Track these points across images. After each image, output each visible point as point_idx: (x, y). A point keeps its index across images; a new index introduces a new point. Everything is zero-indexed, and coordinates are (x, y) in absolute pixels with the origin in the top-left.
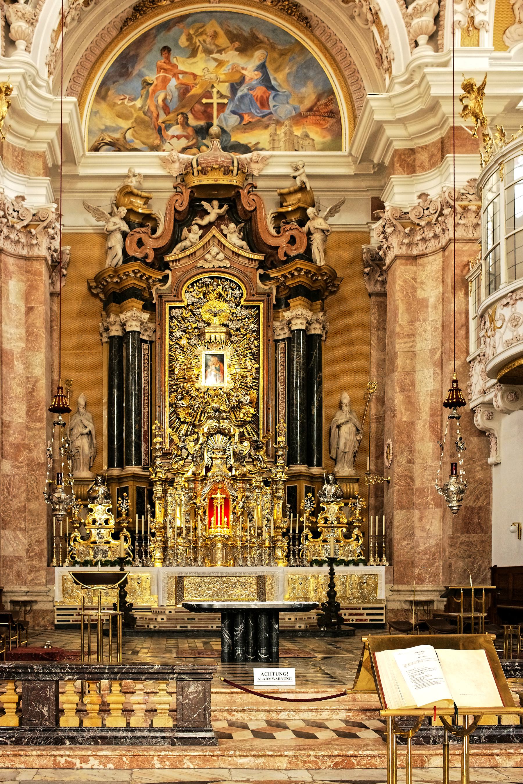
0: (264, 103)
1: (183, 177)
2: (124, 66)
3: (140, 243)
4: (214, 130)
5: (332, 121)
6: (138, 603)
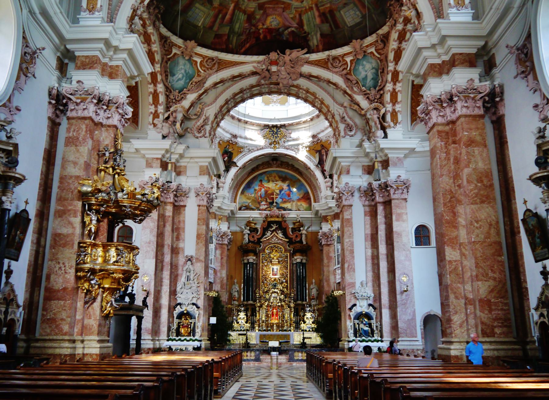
0: (289, 196)
1: (266, 218)
2: (249, 186)
3: (253, 237)
4: (275, 204)
6: (252, 342)
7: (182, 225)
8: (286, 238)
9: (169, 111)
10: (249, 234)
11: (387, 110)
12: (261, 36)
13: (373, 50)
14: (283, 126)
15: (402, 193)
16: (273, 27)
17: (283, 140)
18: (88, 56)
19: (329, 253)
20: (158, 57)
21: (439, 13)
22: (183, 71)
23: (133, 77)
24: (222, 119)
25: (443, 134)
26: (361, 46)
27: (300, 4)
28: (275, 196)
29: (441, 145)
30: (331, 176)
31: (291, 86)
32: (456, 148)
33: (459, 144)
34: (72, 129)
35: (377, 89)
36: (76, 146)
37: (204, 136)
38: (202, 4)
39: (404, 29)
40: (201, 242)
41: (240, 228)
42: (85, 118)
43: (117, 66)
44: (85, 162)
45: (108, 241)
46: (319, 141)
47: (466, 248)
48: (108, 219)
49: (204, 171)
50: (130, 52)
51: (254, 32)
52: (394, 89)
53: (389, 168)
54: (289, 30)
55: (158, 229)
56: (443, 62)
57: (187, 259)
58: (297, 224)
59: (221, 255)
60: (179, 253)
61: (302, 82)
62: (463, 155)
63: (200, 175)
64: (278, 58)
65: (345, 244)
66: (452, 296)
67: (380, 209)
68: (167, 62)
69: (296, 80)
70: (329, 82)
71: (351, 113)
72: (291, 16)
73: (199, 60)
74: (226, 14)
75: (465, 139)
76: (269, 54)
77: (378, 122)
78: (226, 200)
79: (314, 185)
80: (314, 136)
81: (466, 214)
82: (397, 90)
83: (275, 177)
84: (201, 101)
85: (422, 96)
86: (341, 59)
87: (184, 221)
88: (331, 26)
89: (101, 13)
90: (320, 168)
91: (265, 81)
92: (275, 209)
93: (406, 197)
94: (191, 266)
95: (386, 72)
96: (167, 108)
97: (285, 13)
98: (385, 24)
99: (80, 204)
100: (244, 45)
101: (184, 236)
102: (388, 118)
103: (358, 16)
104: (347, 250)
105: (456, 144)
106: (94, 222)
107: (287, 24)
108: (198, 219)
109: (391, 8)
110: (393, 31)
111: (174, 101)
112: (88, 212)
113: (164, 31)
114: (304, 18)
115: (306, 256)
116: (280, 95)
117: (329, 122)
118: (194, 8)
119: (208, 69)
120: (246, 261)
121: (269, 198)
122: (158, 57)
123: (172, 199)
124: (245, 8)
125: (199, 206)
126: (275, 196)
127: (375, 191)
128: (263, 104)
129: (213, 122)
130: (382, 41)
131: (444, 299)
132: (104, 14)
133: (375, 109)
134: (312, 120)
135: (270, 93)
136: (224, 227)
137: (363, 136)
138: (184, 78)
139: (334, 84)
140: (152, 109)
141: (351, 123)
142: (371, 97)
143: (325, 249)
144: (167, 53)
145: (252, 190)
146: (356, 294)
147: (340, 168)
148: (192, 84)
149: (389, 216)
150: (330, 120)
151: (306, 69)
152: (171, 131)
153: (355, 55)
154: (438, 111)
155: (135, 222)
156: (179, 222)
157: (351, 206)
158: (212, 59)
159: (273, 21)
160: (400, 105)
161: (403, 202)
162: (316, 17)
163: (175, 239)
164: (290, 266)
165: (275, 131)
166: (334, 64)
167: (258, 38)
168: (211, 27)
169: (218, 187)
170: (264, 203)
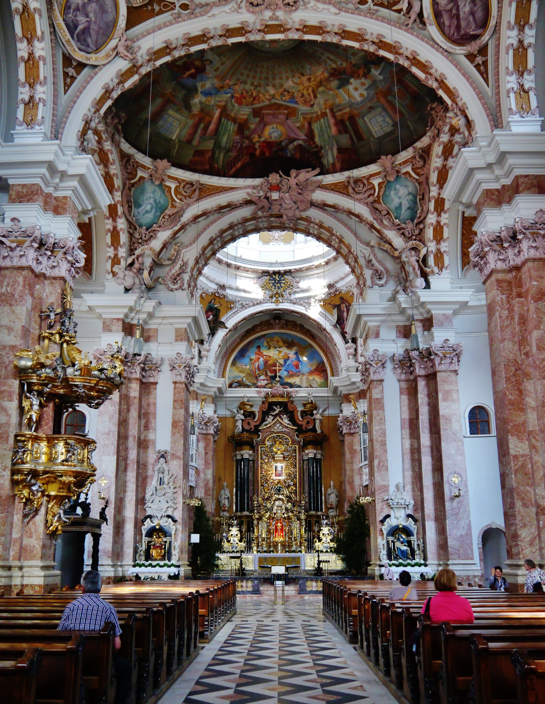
0: (297, 367)
1: (266, 398)
2: (242, 354)
3: (249, 424)
4: (278, 379)
5: (324, 374)
7: (152, 408)
8: (294, 425)
9: (134, 254)
10: (242, 420)
11: (429, 250)
12: (258, 152)
13: (409, 169)
14: (288, 272)
15: (451, 363)
16: (273, 139)
17: (288, 291)
18: (25, 185)
19: (352, 446)
20: (118, 183)
21: (497, 121)
22: (152, 201)
23: (85, 212)
24: (206, 264)
25: (505, 285)
26: (393, 163)
27: (310, 109)
28: (277, 368)
29: (502, 298)
30: (354, 341)
31: (298, 219)
32: (522, 303)
33: (526, 298)
34: (5, 283)
35: (416, 221)
36: (11, 305)
37: (181, 288)
38: (177, 111)
39: (450, 141)
40: (179, 432)
41: (231, 411)
42: (21, 268)
43: (65, 198)
44: (23, 327)
45: (54, 433)
46: (338, 293)
47: (537, 437)
48: (55, 403)
49: (182, 336)
50: (82, 179)
51: (248, 147)
52: (438, 222)
53: (433, 329)
54: (295, 143)
55: (120, 414)
56: (503, 186)
57: (160, 455)
58: (308, 406)
59: (205, 448)
60: (148, 447)
61: (314, 214)
62: (531, 312)
63: (176, 340)
64: (281, 182)
65: (374, 433)
66: (518, 504)
67: (422, 384)
68: (130, 189)
69: (304, 210)
70: (350, 213)
71: (380, 255)
72: (298, 125)
73: (173, 185)
74: (210, 123)
75: (533, 291)
76: (268, 177)
77: (417, 267)
78: (212, 373)
79: (331, 352)
80: (330, 286)
81: (536, 392)
82: (442, 224)
83: (278, 341)
84: (177, 240)
85: (476, 234)
86: (365, 182)
87: (155, 404)
88: (351, 137)
89: (42, 127)
90: (339, 330)
91: (263, 212)
92: (278, 385)
93: (457, 369)
94: (164, 465)
95: (426, 198)
96: (131, 251)
97: (289, 122)
98: (424, 134)
99: (16, 383)
100: (235, 164)
101: (155, 423)
102: (431, 261)
103: (388, 124)
104: (377, 441)
105: (522, 297)
106: (36, 407)
107: (292, 135)
108: (174, 401)
109: (433, 112)
110: (436, 144)
111: (140, 241)
112: (28, 394)
113: (126, 147)
114: (315, 127)
115: (321, 449)
116: (283, 231)
117: (351, 267)
118: (166, 116)
119: (185, 197)
120: (239, 457)
121: (271, 372)
122: (118, 183)
123: (138, 373)
124: (235, 115)
125: (175, 383)
126: (277, 368)
127: (413, 361)
128: (260, 243)
129: (192, 269)
130: (421, 157)
131: (508, 506)
132: (46, 128)
133: (414, 249)
134: (327, 263)
135: (270, 228)
136: (209, 411)
137: (397, 286)
138: (154, 210)
139: (357, 216)
140: (111, 252)
141: (380, 268)
142: (407, 233)
143: (347, 439)
144: (130, 176)
145: (246, 360)
146: (390, 501)
147: (366, 329)
148: (164, 217)
149: (434, 394)
150: (352, 264)
151: (319, 196)
152: (137, 281)
153: (385, 176)
154: (497, 253)
155: (90, 407)
156: (149, 404)
157: (382, 381)
158: (192, 184)
159: (273, 132)
160: (446, 244)
161: (453, 375)
162: (332, 125)
163: (142, 428)
164: (300, 463)
165: (277, 279)
166: (357, 189)
167: (252, 155)
168: (189, 141)
169: (200, 357)
170: (263, 377)
